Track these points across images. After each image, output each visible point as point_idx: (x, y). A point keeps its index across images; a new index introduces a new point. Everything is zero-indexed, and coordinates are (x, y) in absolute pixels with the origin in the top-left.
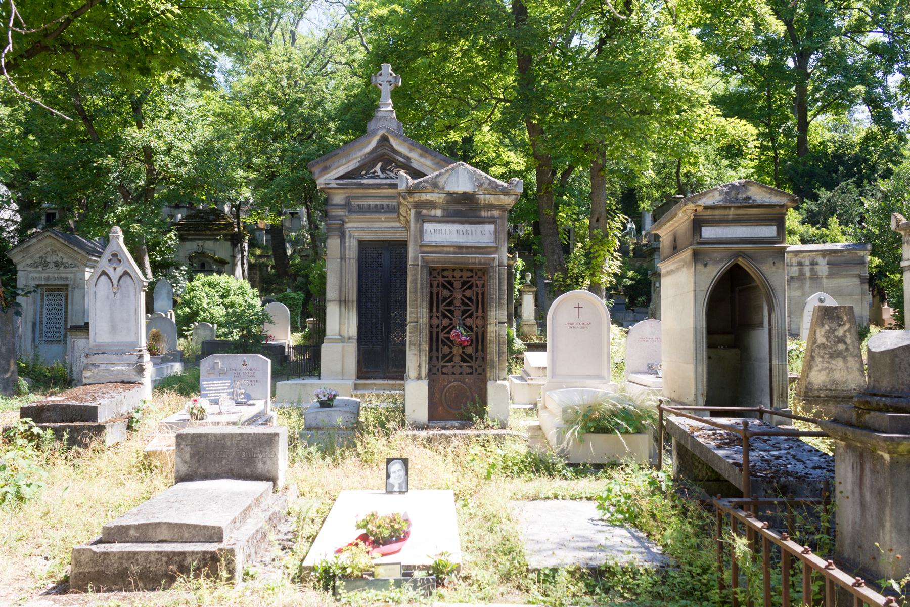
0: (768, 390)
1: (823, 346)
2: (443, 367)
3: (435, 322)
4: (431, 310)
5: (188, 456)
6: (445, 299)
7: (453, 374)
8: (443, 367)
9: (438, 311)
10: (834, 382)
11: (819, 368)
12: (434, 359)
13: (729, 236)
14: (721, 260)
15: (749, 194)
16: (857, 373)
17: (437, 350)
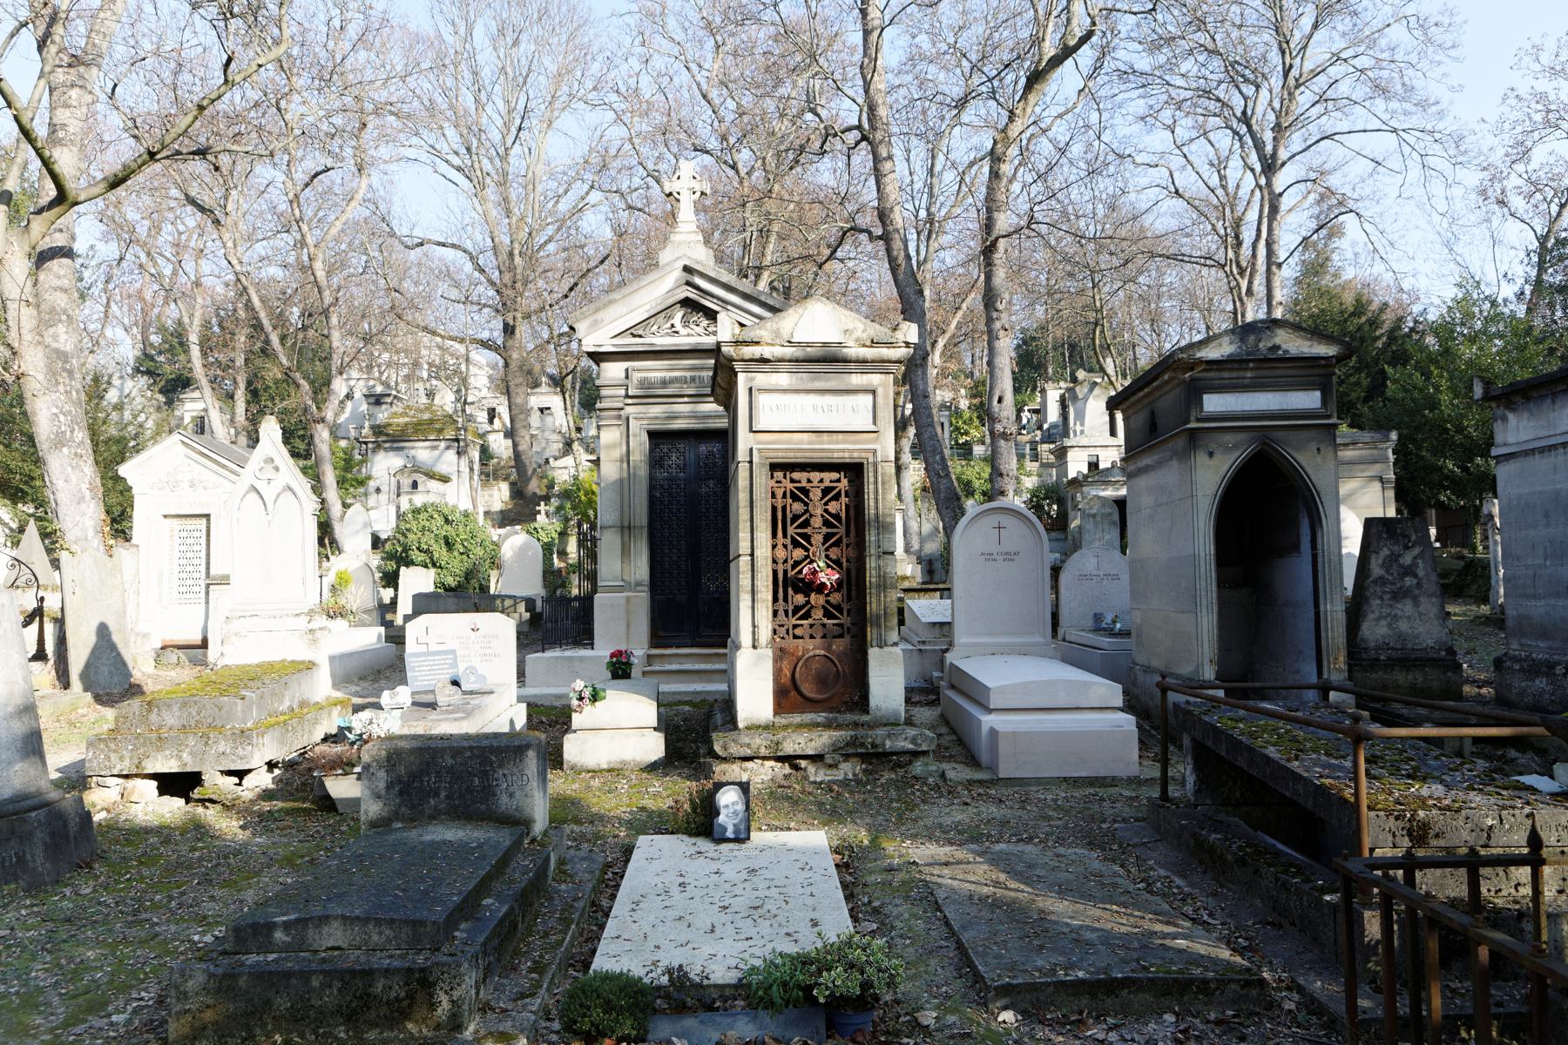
0: (1313, 653)
1: (1381, 581)
2: (795, 626)
3: (781, 554)
4: (774, 535)
5: (382, 785)
6: (795, 518)
7: (812, 637)
8: (795, 626)
9: (785, 536)
10: (1400, 636)
11: (1377, 614)
12: (781, 613)
13: (1247, 408)
14: (1235, 447)
15: (1277, 341)
16: (1436, 623)
17: (786, 600)
